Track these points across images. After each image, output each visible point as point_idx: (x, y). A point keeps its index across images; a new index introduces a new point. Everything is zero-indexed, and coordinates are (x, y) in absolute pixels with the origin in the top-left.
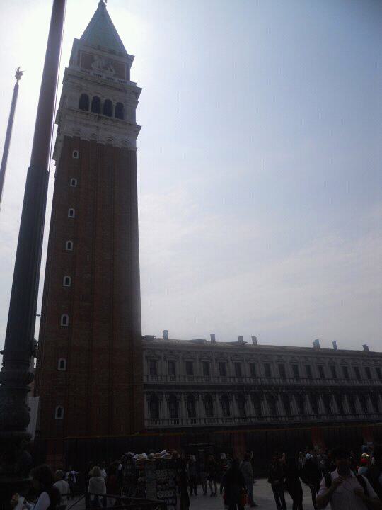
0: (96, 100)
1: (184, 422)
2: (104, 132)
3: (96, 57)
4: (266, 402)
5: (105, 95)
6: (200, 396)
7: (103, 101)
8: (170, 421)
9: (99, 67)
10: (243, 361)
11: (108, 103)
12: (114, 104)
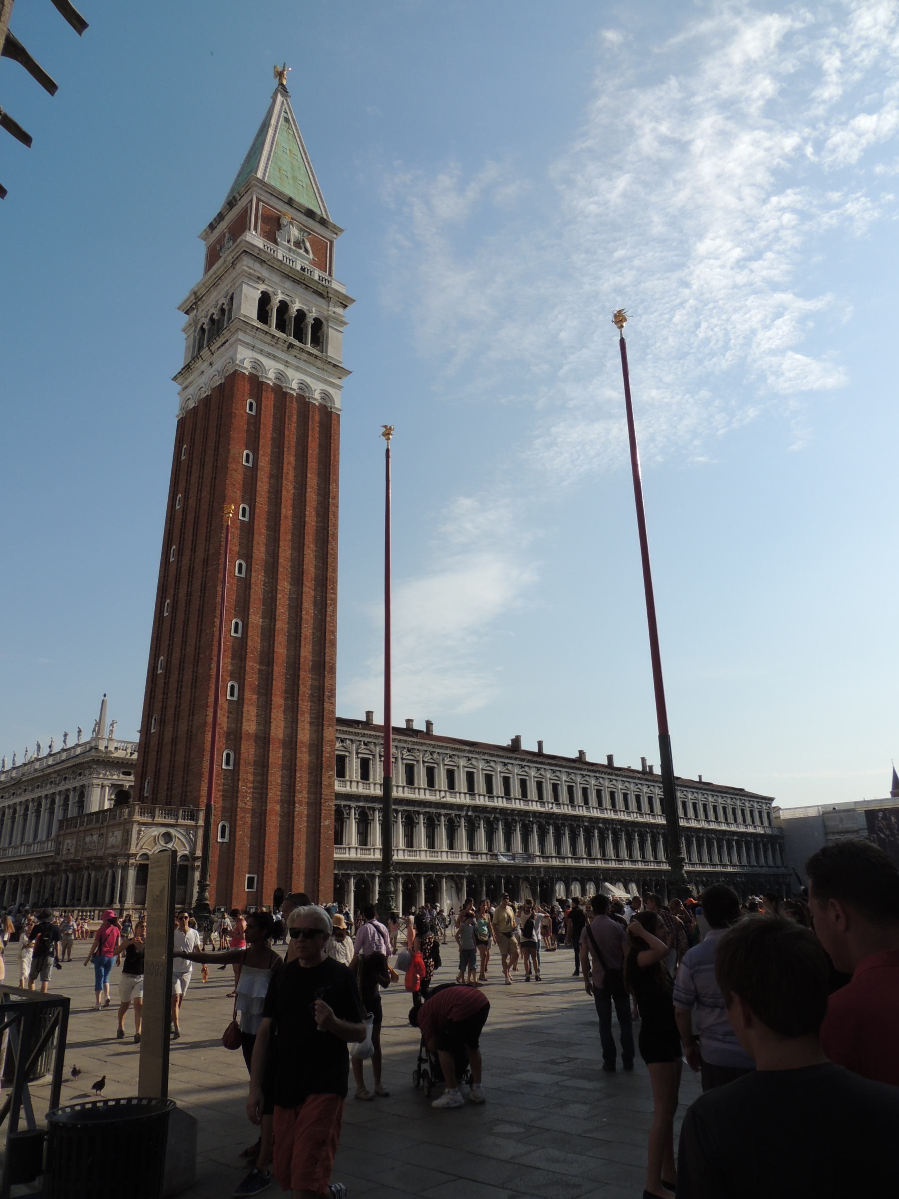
0: (284, 307)
3: (284, 221)
6: (353, 811)
9: (289, 241)
10: (418, 761)
11: (301, 315)
12: (310, 321)
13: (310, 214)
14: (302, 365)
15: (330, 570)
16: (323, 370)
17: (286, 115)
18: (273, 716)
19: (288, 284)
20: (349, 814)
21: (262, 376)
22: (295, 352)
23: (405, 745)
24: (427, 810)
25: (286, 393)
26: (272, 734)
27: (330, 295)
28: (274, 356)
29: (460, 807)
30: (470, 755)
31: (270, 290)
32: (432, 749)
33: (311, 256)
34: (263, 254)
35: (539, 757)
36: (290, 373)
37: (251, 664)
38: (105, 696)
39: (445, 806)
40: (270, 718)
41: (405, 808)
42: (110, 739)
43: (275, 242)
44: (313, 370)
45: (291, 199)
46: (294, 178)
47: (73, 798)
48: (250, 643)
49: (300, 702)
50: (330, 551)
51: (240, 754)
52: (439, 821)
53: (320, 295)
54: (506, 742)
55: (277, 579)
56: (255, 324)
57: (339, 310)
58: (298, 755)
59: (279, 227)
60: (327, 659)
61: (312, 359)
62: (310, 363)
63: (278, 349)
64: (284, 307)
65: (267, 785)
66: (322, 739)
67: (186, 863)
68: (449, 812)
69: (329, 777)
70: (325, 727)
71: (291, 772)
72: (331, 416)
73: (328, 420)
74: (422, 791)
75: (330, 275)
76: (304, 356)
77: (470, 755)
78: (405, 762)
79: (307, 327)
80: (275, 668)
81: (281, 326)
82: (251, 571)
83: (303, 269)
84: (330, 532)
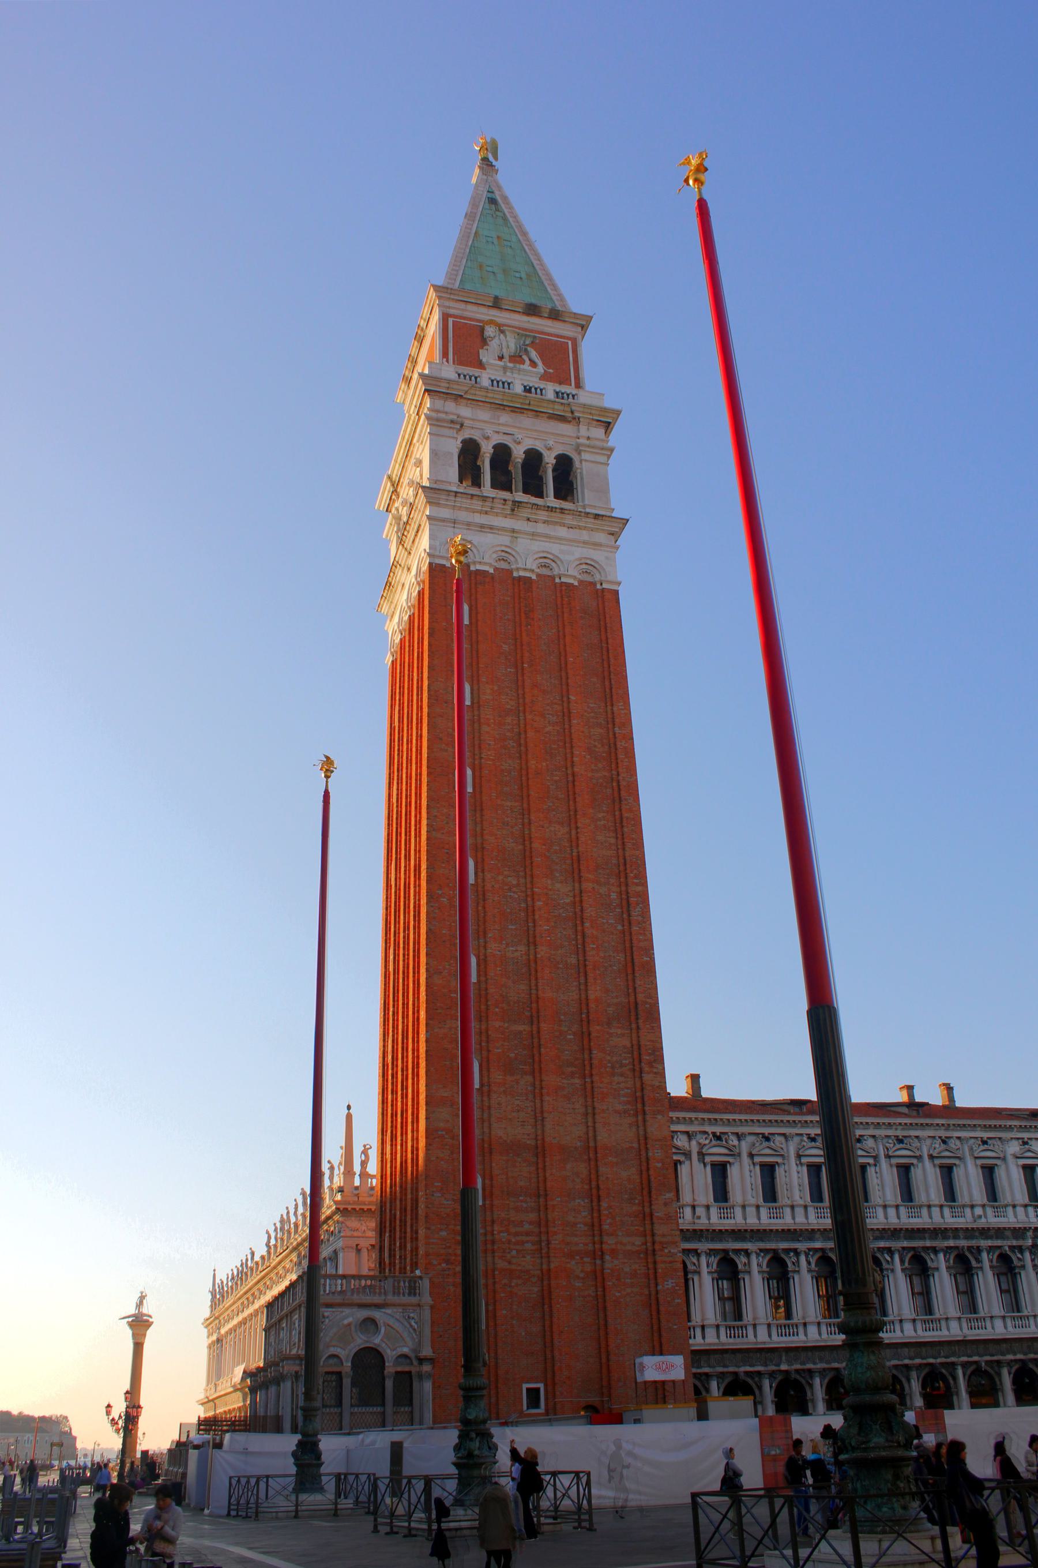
0: (502, 454)
1: (762, 1332)
2: (529, 542)
3: (490, 331)
4: (990, 1274)
6: (803, 1258)
7: (518, 454)
8: (722, 1331)
9: (501, 358)
10: (919, 1158)
11: (533, 458)
12: (550, 459)
14: (541, 528)
15: (629, 845)
16: (580, 528)
17: (490, 195)
18: (546, 1108)
19: (505, 418)
20: (797, 1263)
21: (474, 563)
22: (525, 513)
23: (890, 1132)
24: (951, 1243)
25: (520, 577)
26: (547, 1139)
27: (577, 414)
28: (491, 528)
29: (1019, 1233)
30: (1025, 1135)
31: (476, 436)
32: (943, 1133)
33: (541, 368)
34: (455, 387)
36: (523, 545)
37: (497, 1024)
38: (349, 1107)
39: (985, 1232)
40: (542, 1112)
41: (906, 1244)
43: (481, 366)
44: (562, 532)
45: (496, 298)
46: (505, 271)
48: (491, 991)
49: (596, 1078)
50: (625, 815)
51: (491, 1179)
52: (978, 1261)
53: (562, 419)
55: (532, 876)
56: (455, 489)
57: (599, 432)
58: (602, 1169)
59: (484, 342)
60: (640, 997)
61: (556, 517)
62: (556, 523)
63: (497, 514)
64: (502, 454)
65: (547, 1226)
66: (646, 1138)
67: (407, 1369)
68: (999, 1243)
69: (666, 1204)
70: (648, 1117)
71: (592, 1201)
72: (603, 597)
74: (936, 1211)
75: (578, 386)
76: (543, 515)
77: (1025, 1135)
78: (894, 1161)
79: (545, 472)
80: (542, 1025)
81: (501, 481)
82: (483, 871)
83: (528, 390)
84: (623, 783)
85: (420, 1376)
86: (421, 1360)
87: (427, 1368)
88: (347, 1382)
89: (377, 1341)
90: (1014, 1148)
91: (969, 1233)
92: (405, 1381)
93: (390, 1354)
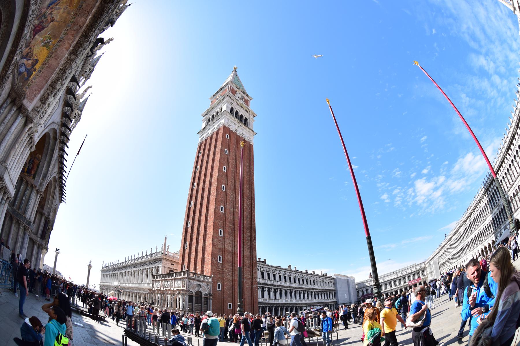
0: (237, 113)
3: (237, 92)
5: (241, 112)
7: (240, 114)
11: (242, 116)
13: (244, 93)
35: (296, 271)
39: (273, 285)
42: (168, 251)
47: (154, 271)
53: (247, 112)
54: (286, 267)
73: (249, 148)
85: (210, 299)
86: (210, 295)
87: (211, 297)
88: (194, 298)
89: (201, 289)
90: (278, 272)
91: (271, 285)
92: (207, 299)
93: (204, 293)
